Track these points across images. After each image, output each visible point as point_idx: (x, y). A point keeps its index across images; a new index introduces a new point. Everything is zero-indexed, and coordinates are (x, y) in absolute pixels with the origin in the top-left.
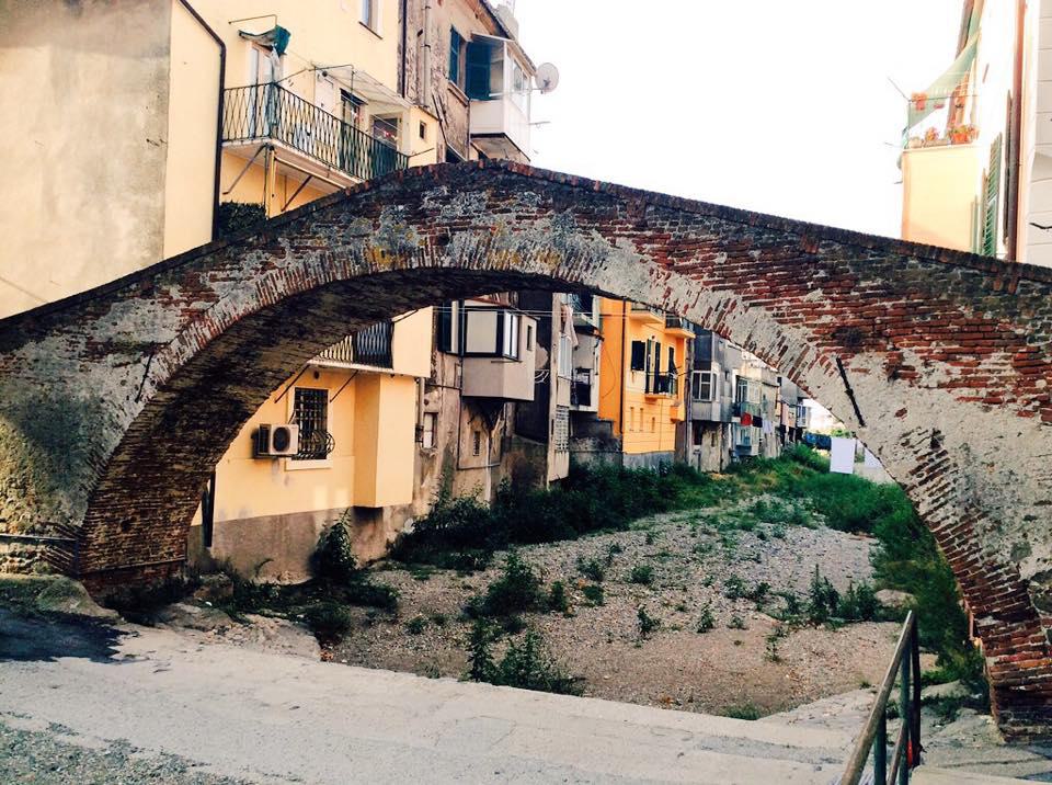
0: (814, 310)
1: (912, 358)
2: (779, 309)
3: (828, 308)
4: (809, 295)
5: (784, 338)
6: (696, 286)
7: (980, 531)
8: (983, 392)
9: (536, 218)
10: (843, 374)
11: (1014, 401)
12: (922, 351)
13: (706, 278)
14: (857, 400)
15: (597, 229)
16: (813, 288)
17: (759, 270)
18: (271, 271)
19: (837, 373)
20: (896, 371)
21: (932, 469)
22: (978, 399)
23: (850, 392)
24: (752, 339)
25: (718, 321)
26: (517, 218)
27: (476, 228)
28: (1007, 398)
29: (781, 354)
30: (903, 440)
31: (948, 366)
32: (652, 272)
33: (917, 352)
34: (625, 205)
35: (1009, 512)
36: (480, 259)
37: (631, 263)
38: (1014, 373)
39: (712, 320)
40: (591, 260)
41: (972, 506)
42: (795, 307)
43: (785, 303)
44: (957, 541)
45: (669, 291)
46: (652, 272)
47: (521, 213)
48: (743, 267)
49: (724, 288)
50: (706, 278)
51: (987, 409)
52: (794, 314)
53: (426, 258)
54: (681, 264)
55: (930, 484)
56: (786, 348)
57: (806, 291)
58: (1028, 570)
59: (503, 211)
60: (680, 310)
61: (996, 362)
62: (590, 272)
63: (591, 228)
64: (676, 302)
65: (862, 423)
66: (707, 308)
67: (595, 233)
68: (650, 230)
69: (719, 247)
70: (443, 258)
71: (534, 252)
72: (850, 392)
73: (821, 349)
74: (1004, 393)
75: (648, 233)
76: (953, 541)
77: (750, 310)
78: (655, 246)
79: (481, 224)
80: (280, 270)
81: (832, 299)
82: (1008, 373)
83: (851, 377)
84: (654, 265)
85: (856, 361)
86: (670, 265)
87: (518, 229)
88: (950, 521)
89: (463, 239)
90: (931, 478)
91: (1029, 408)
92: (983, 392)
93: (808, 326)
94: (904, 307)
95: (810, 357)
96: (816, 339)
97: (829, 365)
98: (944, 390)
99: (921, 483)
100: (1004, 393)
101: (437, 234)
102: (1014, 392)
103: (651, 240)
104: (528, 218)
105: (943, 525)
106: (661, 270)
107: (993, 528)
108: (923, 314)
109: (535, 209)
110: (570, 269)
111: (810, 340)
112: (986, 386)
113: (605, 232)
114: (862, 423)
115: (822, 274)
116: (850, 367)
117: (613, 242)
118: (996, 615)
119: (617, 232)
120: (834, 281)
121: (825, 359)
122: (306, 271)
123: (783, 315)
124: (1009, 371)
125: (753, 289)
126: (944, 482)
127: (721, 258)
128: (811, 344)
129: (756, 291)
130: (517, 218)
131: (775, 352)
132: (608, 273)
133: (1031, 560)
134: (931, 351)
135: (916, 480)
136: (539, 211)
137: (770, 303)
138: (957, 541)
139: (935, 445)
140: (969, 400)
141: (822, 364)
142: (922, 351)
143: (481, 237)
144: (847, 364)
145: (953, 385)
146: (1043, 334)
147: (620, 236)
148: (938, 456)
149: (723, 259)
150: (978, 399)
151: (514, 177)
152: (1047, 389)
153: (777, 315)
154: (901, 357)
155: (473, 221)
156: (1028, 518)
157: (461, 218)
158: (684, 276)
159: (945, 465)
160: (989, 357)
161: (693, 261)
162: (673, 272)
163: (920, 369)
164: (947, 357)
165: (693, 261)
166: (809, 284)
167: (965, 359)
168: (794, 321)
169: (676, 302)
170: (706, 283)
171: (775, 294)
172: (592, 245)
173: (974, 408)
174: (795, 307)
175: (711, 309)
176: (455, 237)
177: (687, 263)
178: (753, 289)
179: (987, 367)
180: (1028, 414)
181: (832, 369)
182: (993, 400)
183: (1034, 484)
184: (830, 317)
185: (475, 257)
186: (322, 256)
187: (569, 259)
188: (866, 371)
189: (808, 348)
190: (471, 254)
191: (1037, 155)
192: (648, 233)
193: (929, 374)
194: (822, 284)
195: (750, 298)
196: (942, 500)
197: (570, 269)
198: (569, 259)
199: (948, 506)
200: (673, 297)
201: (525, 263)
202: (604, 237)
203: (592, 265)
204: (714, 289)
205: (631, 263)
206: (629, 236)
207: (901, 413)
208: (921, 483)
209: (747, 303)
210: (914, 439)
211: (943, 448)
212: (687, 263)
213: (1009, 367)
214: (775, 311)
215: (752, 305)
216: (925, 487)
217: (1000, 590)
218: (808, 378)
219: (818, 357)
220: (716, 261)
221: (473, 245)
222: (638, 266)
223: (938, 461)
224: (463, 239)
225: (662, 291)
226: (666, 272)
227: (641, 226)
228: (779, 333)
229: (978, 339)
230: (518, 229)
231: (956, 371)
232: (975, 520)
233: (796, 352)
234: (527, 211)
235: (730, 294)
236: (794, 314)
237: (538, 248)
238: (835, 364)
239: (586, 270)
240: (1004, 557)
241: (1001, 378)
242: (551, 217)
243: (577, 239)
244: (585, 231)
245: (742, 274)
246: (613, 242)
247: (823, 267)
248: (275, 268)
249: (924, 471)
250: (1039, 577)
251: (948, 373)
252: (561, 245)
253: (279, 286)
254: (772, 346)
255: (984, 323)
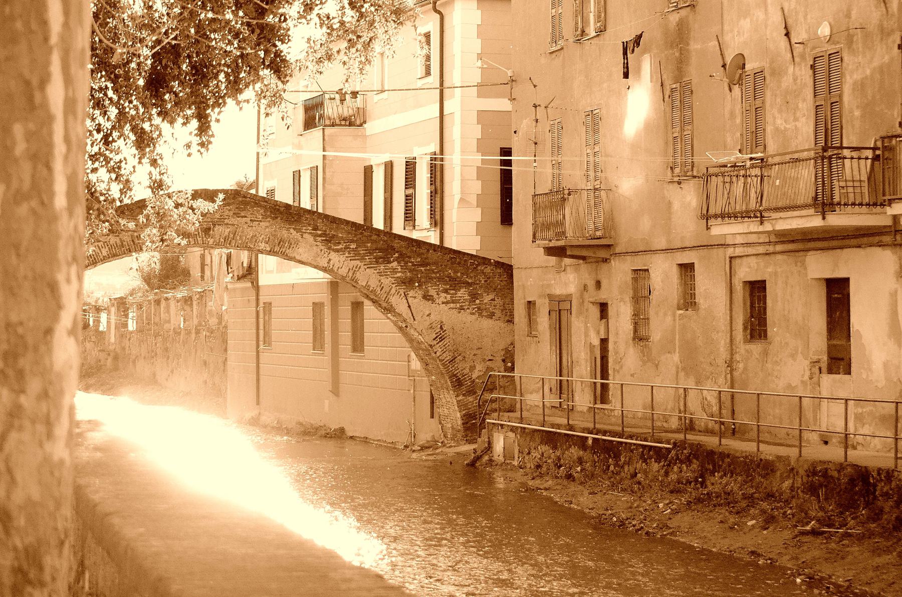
0: (394, 271)
1: (432, 292)
2: (379, 270)
3: (400, 270)
4: (392, 264)
5: (382, 283)
6: (342, 258)
7: (459, 361)
8: (458, 305)
9: (261, 221)
10: (407, 300)
11: (468, 309)
12: (436, 289)
13: (347, 255)
14: (412, 309)
15: (293, 228)
16: (393, 261)
17: (370, 252)
18: (97, 243)
19: (404, 298)
20: (427, 297)
21: (441, 337)
22: (456, 308)
23: (409, 307)
24: (369, 283)
25: (353, 274)
26: (251, 220)
27: (227, 224)
28: (466, 307)
29: (381, 290)
30: (430, 326)
31: (445, 295)
32: (321, 250)
33: (434, 289)
34: (307, 218)
35: (468, 353)
36: (230, 241)
37: (311, 246)
38: (468, 298)
39: (350, 274)
40: (291, 244)
41: (456, 351)
42: (386, 269)
43: (382, 267)
44: (451, 366)
45: (330, 260)
46: (321, 250)
47: (252, 219)
48: (363, 250)
49: (355, 260)
50: (347, 255)
51: (459, 312)
52: (386, 272)
53: (199, 239)
54: (335, 248)
55: (440, 344)
56: (383, 287)
57: (389, 262)
58: (474, 376)
59: (242, 217)
60: (335, 270)
61: (463, 294)
62: (291, 249)
63: (290, 228)
64: (333, 266)
65: (414, 320)
66: (348, 268)
67: (292, 231)
68: (320, 230)
69: (352, 241)
70: (209, 239)
71: (261, 238)
72: (409, 307)
73: (397, 288)
74: (465, 306)
75: (319, 232)
76: (449, 366)
77: (367, 270)
78: (323, 238)
79: (230, 223)
80: (104, 243)
81: (401, 266)
82: (466, 298)
83: (410, 300)
84: (323, 248)
85: (411, 293)
86: (329, 248)
87: (252, 226)
88: (448, 358)
89: (220, 230)
90: (441, 341)
91: (474, 311)
92: (458, 305)
93: (391, 277)
94: (429, 270)
95: (393, 291)
96: (395, 283)
97: (401, 295)
98: (444, 305)
99: (437, 344)
100: (465, 306)
101: (205, 226)
102: (469, 305)
103: (320, 236)
104: (258, 221)
105: (445, 360)
106: (326, 250)
107: (463, 360)
108: (436, 273)
109: (261, 217)
110: (280, 248)
111: (393, 284)
112: (459, 303)
113: (298, 230)
114: (414, 320)
115: (397, 255)
116: (410, 295)
117: (302, 235)
118: (464, 395)
119: (304, 231)
120: (402, 257)
121: (399, 292)
122: (122, 244)
123: (381, 272)
124: (467, 297)
125: (368, 260)
126: (445, 343)
127: (353, 246)
128: (393, 286)
129: (370, 262)
130: (251, 220)
131: (379, 289)
132: (300, 250)
133: (476, 371)
134: (439, 289)
135: (435, 342)
136: (262, 218)
137: (377, 267)
138: (451, 366)
139: (441, 327)
140: (453, 308)
141: (398, 294)
142: (436, 289)
143: (231, 229)
144: (408, 294)
145: (447, 303)
146: (478, 282)
147: (305, 233)
148: (443, 332)
149: (355, 247)
150: (456, 308)
151: (248, 199)
152: (480, 304)
153: (379, 273)
154: (428, 291)
155: (226, 221)
156: (475, 355)
157: (218, 219)
158: (337, 253)
159: (445, 336)
160: (460, 291)
161: (341, 246)
162: (331, 251)
163: (435, 296)
164: (446, 291)
165: (341, 246)
166: (392, 259)
167: (452, 292)
168: (386, 275)
169: (333, 266)
170: (347, 257)
171: (377, 262)
172: (291, 237)
173: (455, 311)
174: (386, 269)
175: (349, 269)
176: (216, 229)
177: (338, 247)
178: (368, 260)
179: (460, 295)
180: (473, 314)
181: (402, 297)
182: (462, 308)
183: (476, 341)
184: (400, 274)
185: (228, 239)
186: (132, 236)
187: (280, 242)
188: (415, 297)
189: (392, 287)
190: (225, 238)
191: (461, 200)
192: (319, 232)
193: (439, 298)
194: (397, 259)
195: (368, 265)
196: (445, 350)
197: (280, 248)
198: (280, 242)
199: (447, 352)
200: (331, 262)
201: (256, 244)
202: (297, 232)
203: (292, 246)
204: (351, 260)
205: (311, 246)
206: (310, 233)
207: (429, 315)
208: (437, 344)
209: (366, 267)
210: (434, 325)
211: (445, 329)
212: (338, 247)
213: (467, 295)
214: (378, 271)
215: (368, 268)
216: (439, 345)
217: (466, 384)
218: (393, 300)
219: (396, 291)
220: (351, 247)
221: (226, 233)
222: (315, 248)
223: (443, 334)
224: (220, 230)
225: (326, 260)
226: (328, 251)
227: (315, 229)
228: (380, 281)
229: (455, 284)
230: (252, 226)
231: (449, 296)
232: (456, 357)
233: (386, 289)
234: (256, 217)
235: (358, 262)
236: (386, 272)
237: (263, 236)
238: (403, 295)
239: (289, 249)
240: (467, 371)
241: (464, 300)
242: (269, 221)
243: (284, 234)
244: (288, 229)
245: (364, 253)
246: (302, 235)
247: (397, 252)
248: (100, 241)
249: (438, 338)
250: (478, 377)
251: (446, 298)
252: (275, 236)
253: (103, 252)
254: (377, 286)
255: (458, 277)
